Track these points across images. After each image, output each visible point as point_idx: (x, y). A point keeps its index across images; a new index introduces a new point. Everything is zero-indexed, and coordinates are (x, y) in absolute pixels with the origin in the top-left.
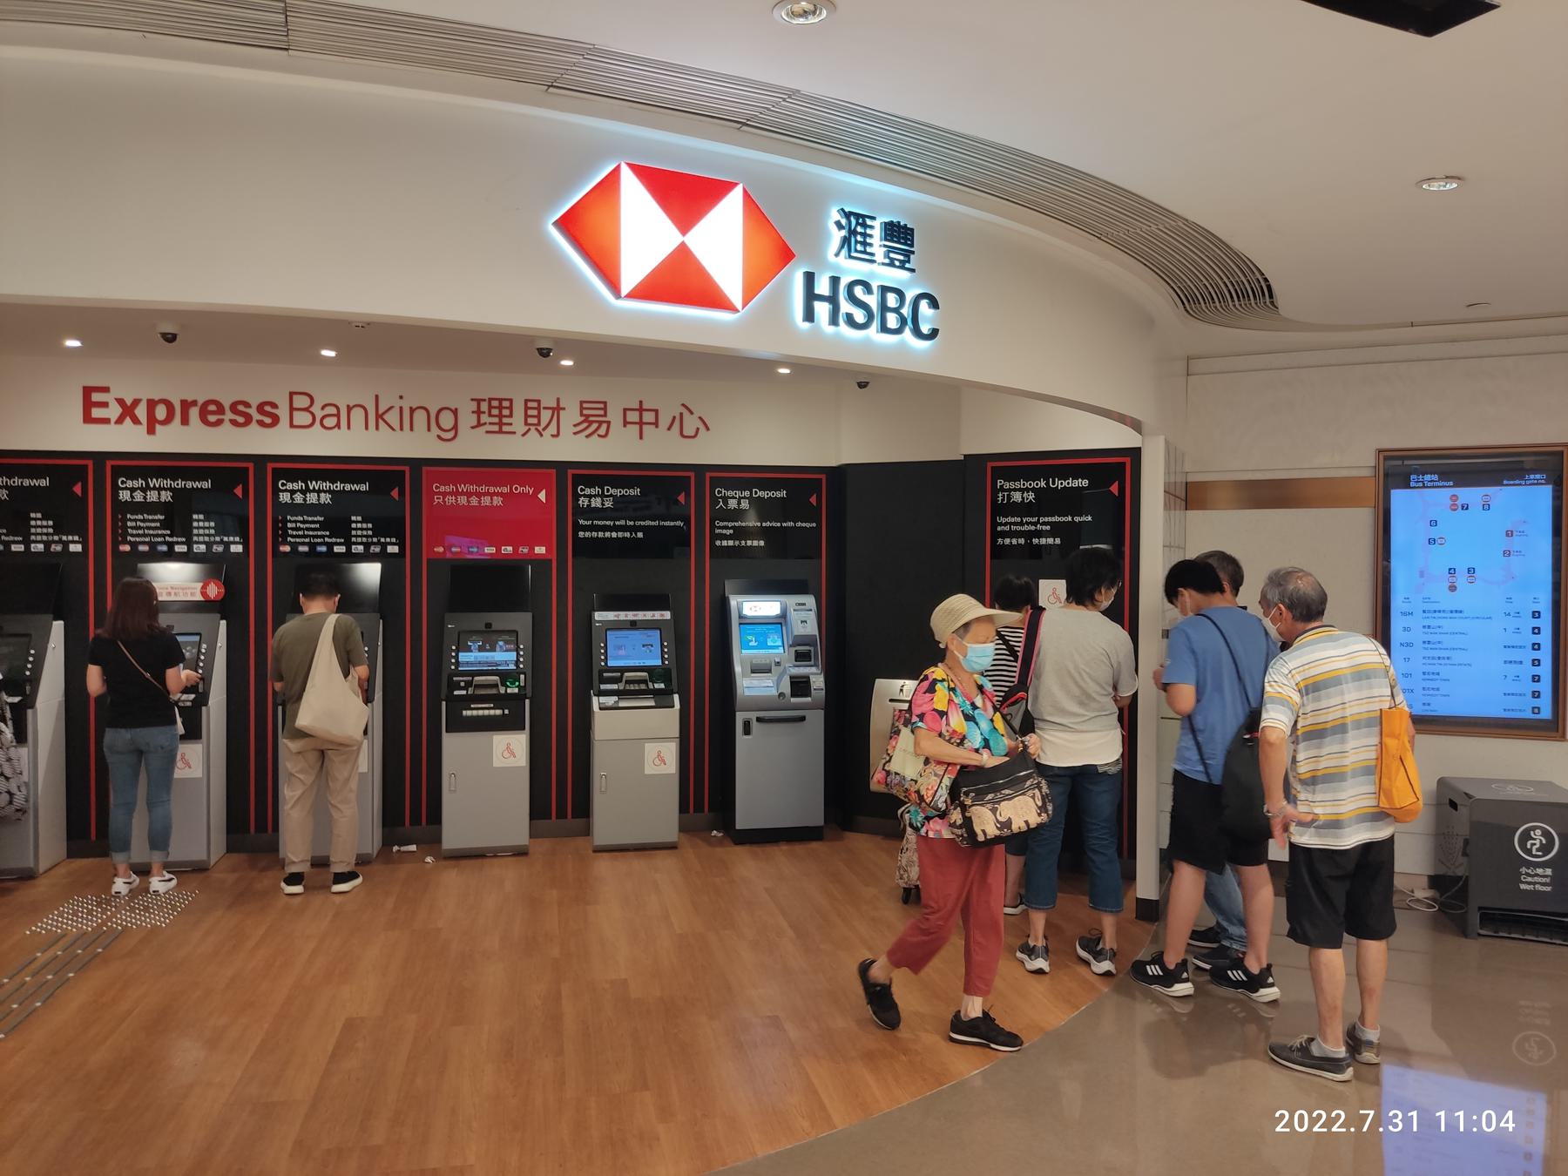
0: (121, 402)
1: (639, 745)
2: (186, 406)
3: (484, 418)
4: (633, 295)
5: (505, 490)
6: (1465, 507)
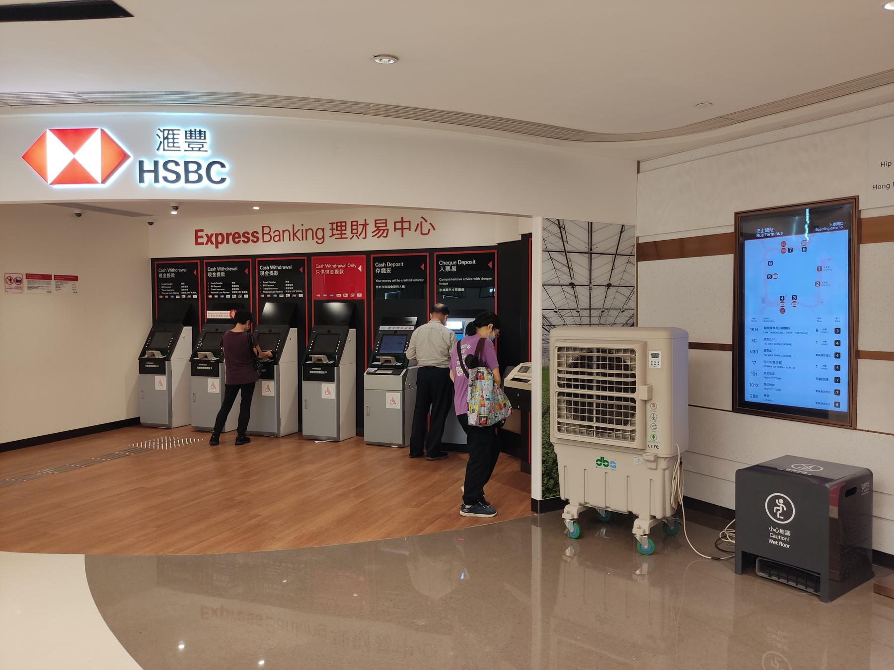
0: (207, 235)
1: (389, 395)
2: (228, 235)
3: (335, 232)
4: (104, 181)
5: (345, 266)
6: (790, 250)
